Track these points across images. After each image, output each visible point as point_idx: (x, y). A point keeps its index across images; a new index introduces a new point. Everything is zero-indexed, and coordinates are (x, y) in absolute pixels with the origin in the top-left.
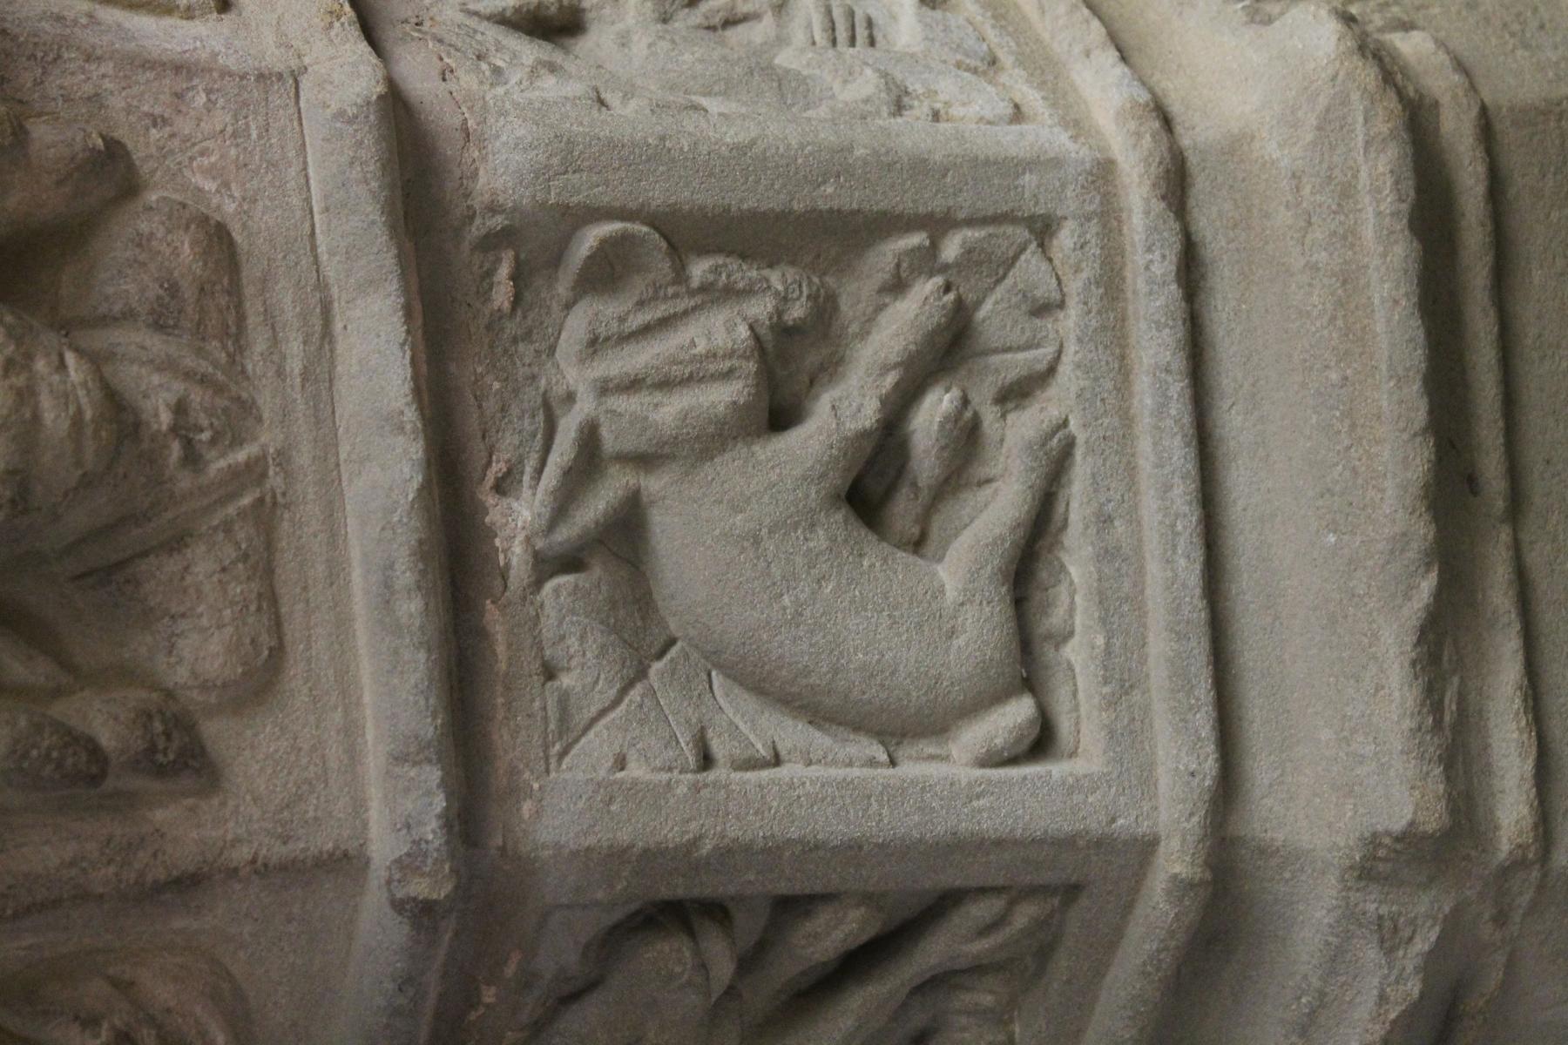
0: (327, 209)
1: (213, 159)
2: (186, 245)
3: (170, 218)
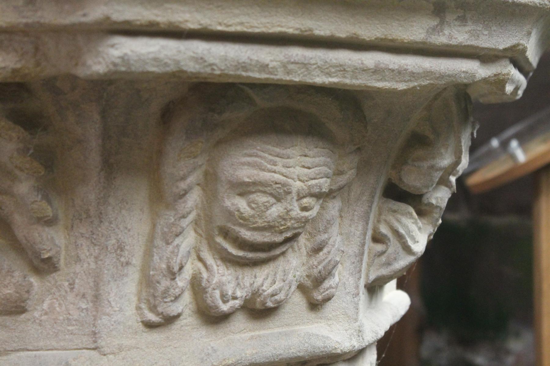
0: (35, 356)
1: (58, 309)
2: (9, 291)
3: (20, 285)
